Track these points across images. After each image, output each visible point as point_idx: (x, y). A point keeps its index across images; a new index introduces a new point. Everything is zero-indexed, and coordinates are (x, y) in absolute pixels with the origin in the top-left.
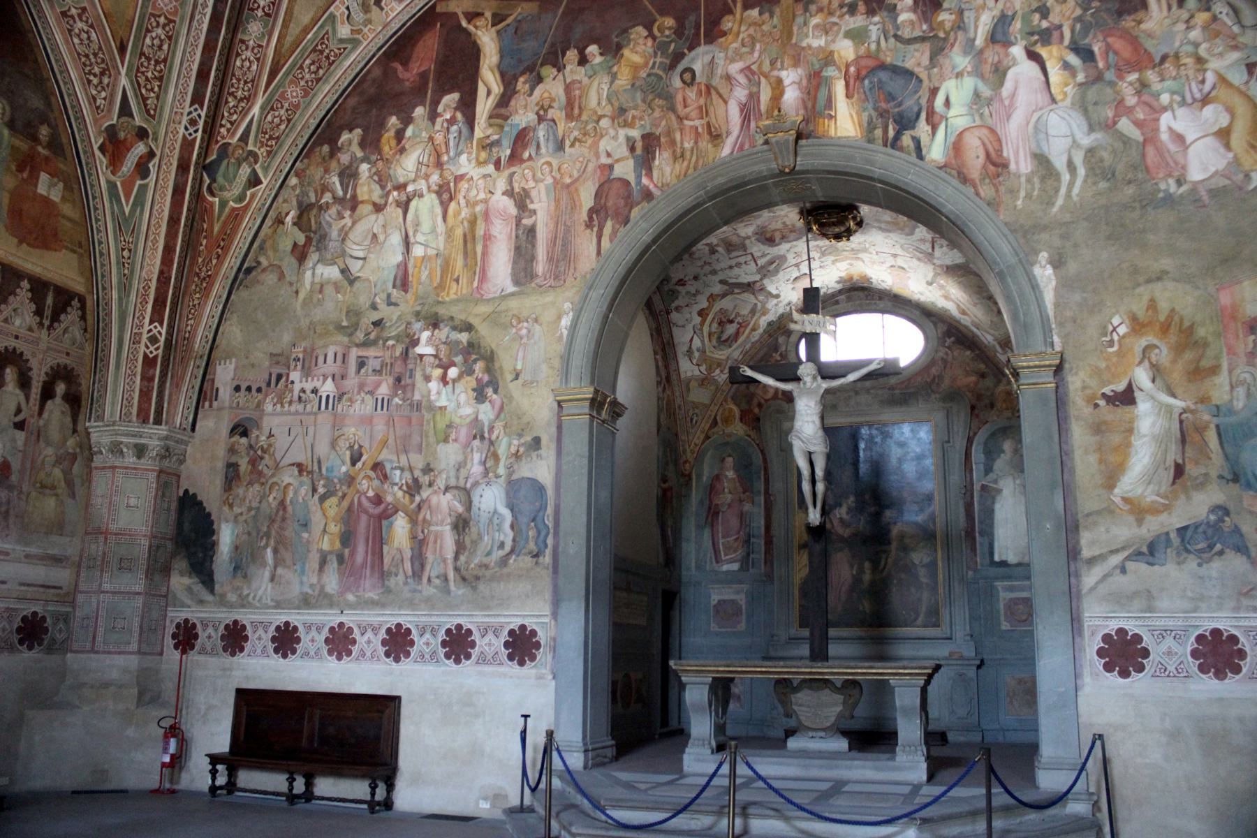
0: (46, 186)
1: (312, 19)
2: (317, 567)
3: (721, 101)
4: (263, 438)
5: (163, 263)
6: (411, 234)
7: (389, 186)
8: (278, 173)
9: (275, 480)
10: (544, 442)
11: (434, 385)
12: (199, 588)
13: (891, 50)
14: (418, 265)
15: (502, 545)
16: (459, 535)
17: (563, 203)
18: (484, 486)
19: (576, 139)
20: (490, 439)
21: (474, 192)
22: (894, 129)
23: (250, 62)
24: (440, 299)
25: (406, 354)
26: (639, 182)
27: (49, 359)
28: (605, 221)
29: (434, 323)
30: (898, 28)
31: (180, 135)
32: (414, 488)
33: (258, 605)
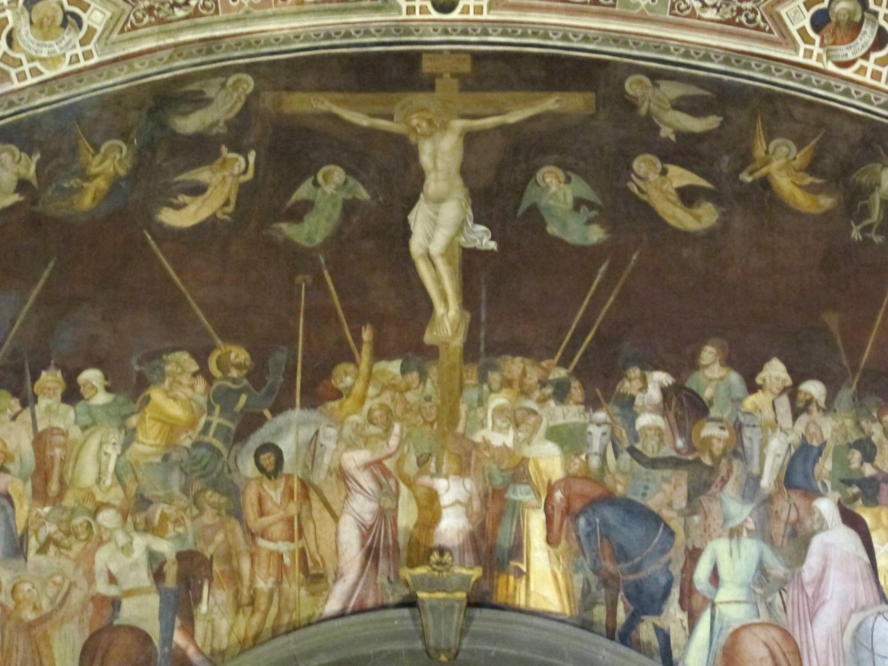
3: (327, 515)
13: (623, 473)
19: (49, 539)
22: (626, 610)
26: (167, 639)
30: (636, 439)
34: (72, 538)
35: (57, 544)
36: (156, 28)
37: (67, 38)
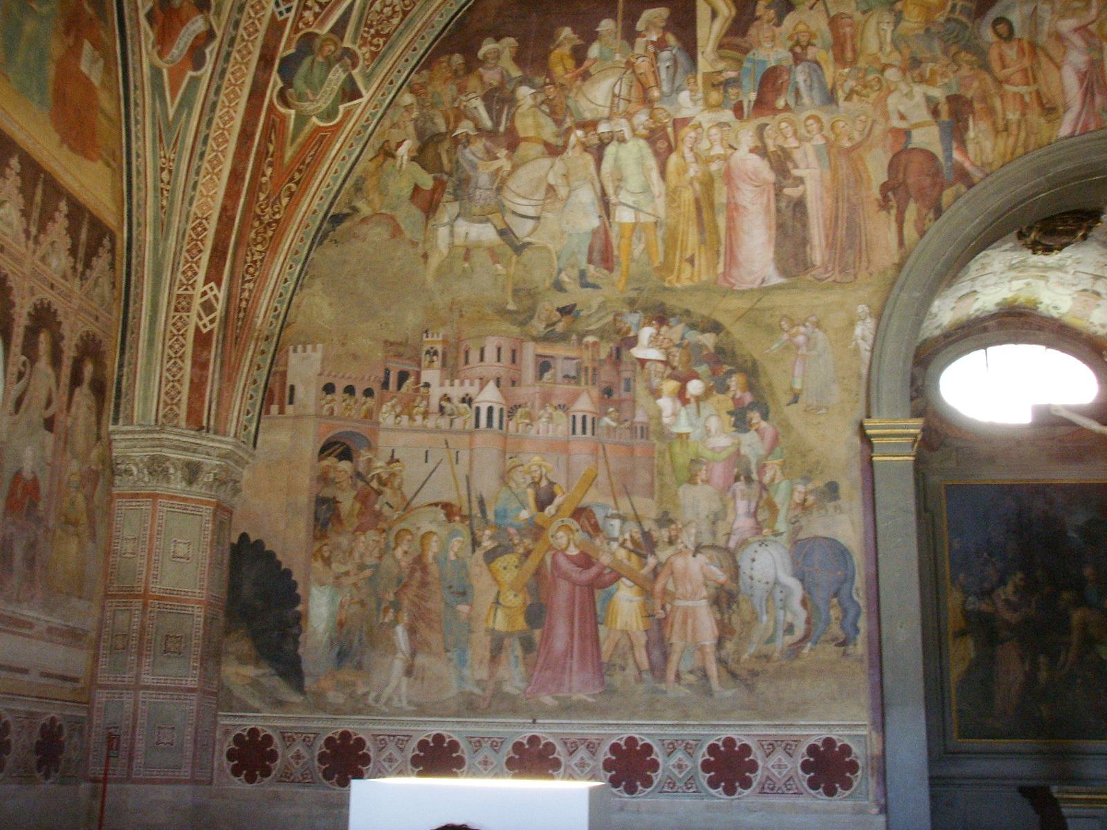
2: (487, 654)
6: (610, 191)
7: (568, 122)
8: (386, 84)
9: (404, 525)
10: (844, 489)
14: (627, 234)
15: (790, 629)
18: (756, 546)
20: (760, 482)
21: (705, 145)
24: (667, 285)
25: (617, 357)
28: (907, 202)
29: (661, 317)
31: (268, 13)
32: (645, 545)
33: (384, 709)
35: (858, 93)
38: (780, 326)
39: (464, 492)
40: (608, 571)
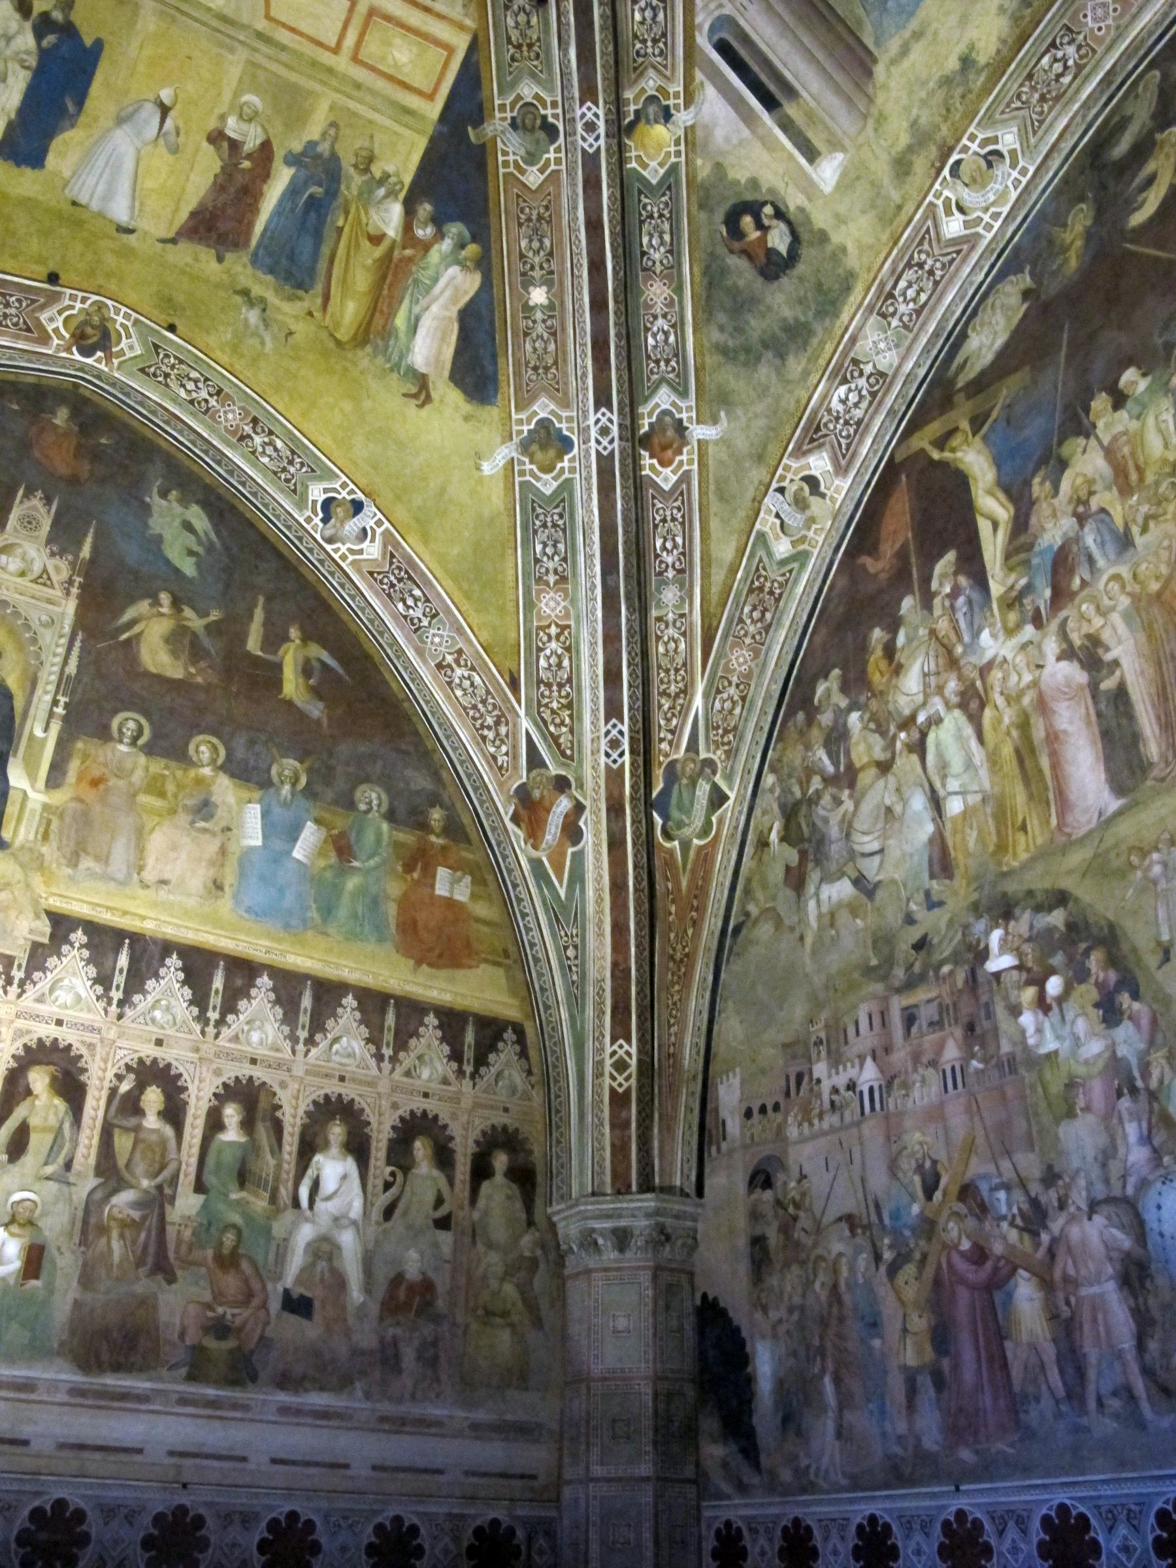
0: (444, 883)
1: (737, 551)
4: (793, 1184)
5: (615, 948)
6: (938, 785)
7: (893, 729)
11: (1027, 1019)
12: (738, 1461)
16: (1136, 1298)
17: (1158, 627)
18: (1159, 1185)
20: (1147, 1089)
21: (1014, 678)
23: (676, 641)
24: (1005, 869)
27: (477, 1122)
29: (1004, 911)
31: (603, 766)
34: (1164, 504)
35: (1154, 517)
36: (1058, 107)
37: (999, 173)
38: (1130, 864)
39: (860, 1195)
40: (1002, 1263)
